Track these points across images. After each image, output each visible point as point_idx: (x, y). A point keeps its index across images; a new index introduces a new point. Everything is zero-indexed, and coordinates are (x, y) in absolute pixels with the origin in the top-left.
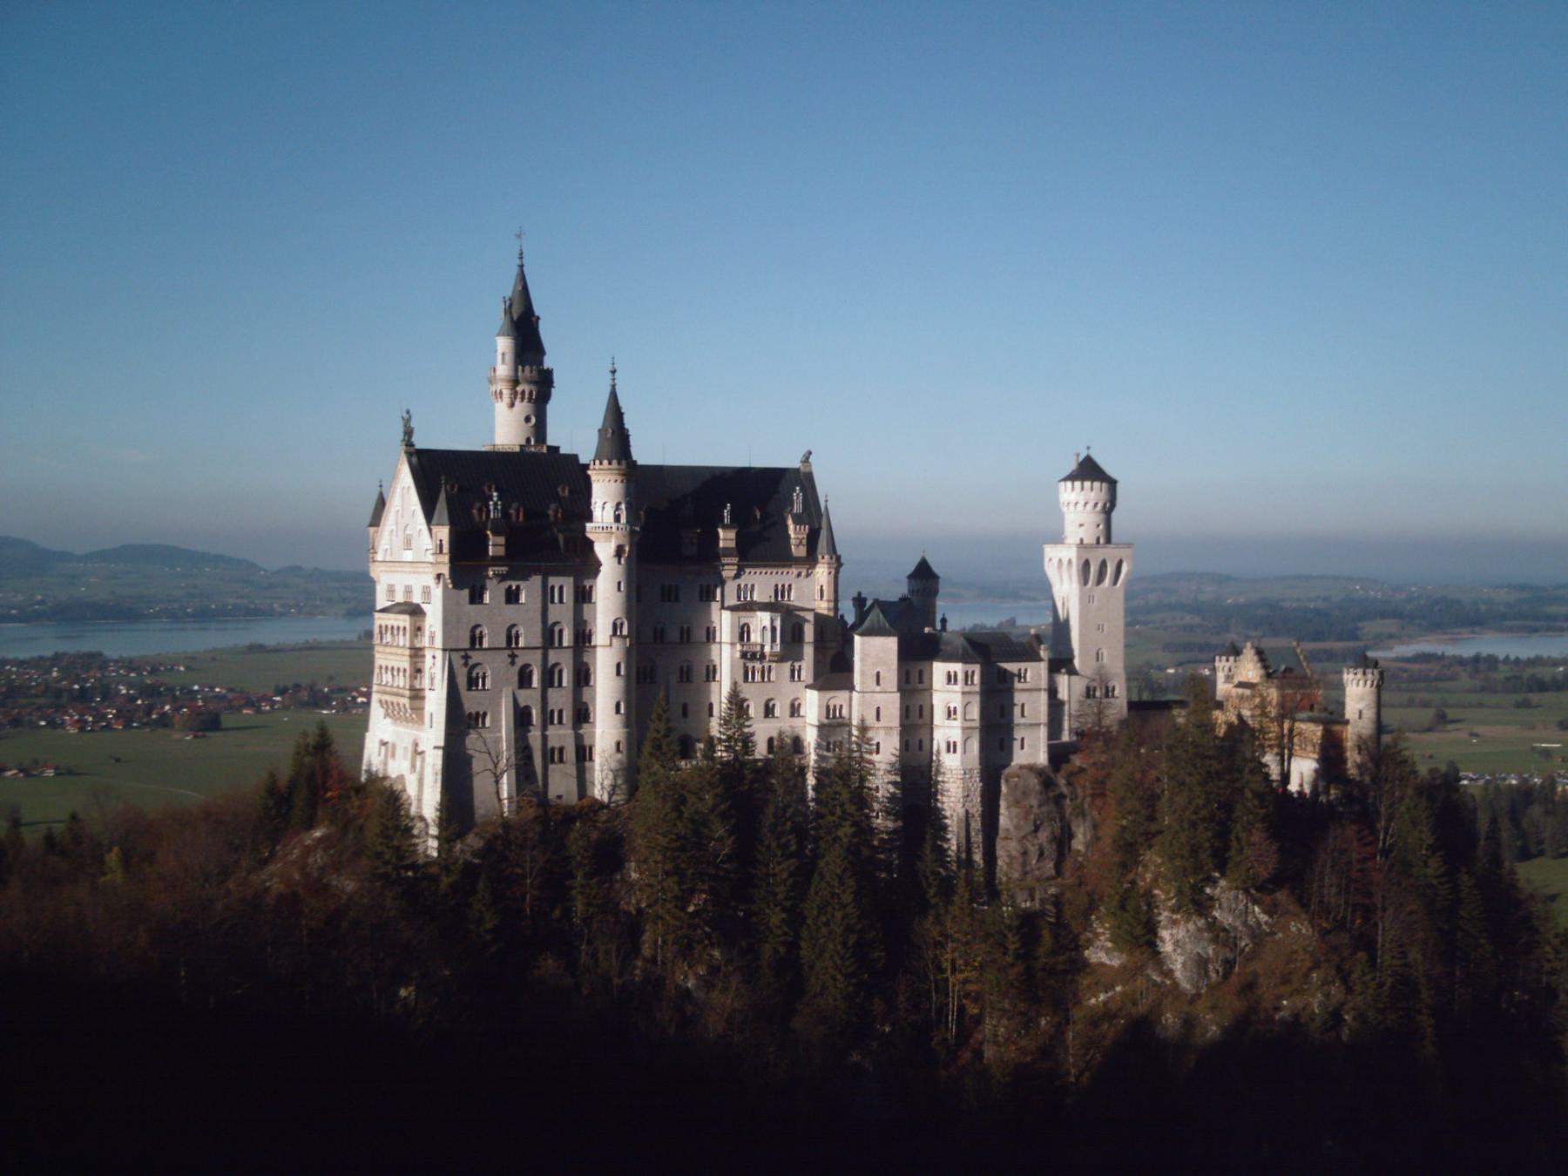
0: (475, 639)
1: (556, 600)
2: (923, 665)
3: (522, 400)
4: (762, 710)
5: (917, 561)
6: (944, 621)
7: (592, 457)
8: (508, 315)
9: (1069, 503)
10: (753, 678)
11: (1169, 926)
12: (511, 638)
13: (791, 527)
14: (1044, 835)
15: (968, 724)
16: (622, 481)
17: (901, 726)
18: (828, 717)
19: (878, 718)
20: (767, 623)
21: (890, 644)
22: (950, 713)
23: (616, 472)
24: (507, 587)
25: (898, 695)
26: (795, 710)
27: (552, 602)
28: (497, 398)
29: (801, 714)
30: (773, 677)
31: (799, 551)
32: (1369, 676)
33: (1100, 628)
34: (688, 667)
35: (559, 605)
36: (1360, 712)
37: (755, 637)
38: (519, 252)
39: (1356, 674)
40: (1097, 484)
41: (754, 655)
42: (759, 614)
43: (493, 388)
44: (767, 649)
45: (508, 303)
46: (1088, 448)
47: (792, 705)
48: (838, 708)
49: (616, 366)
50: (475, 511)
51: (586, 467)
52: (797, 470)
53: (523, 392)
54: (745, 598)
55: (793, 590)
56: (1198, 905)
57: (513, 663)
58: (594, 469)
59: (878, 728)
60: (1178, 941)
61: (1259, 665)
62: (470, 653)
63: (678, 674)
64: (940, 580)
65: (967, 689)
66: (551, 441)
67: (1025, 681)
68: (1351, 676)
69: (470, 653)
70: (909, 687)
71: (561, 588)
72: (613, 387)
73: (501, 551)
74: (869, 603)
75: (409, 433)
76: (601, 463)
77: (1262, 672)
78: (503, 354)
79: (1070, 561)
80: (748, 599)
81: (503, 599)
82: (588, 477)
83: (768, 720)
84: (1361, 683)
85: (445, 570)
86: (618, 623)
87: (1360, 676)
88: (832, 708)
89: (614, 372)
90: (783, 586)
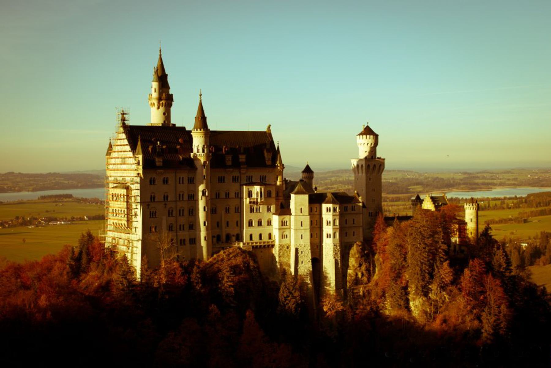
0: (153, 198)
1: (181, 182)
2: (317, 205)
3: (162, 106)
4: (257, 223)
5: (304, 167)
6: (316, 189)
7: (193, 128)
8: (156, 74)
9: (361, 144)
10: (253, 211)
11: (412, 300)
12: (166, 198)
13: (266, 154)
14: (363, 268)
15: (335, 227)
16: (203, 137)
17: (310, 228)
18: (282, 226)
19: (302, 226)
20: (259, 190)
21: (305, 198)
22: (328, 223)
23: (202, 133)
24: (163, 177)
25: (309, 217)
26: (269, 223)
27: (180, 183)
28: (152, 105)
29: (272, 224)
30: (261, 211)
31: (269, 163)
32: (475, 206)
33: (373, 190)
34: (229, 207)
35: (182, 185)
36: (471, 219)
37: (254, 196)
38: (159, 50)
39: (469, 205)
40: (372, 136)
41: (254, 203)
42: (256, 187)
43: (151, 102)
44: (259, 200)
45: (156, 69)
46: (368, 123)
47: (268, 221)
48: (285, 222)
49: (201, 93)
50: (150, 149)
51: (190, 132)
52: (265, 132)
53: (163, 103)
54: (249, 180)
55: (267, 179)
56: (425, 292)
57: (165, 207)
58: (194, 132)
59: (303, 229)
60: (416, 306)
61: (432, 203)
62: (150, 203)
63: (225, 210)
64: (314, 173)
65: (334, 214)
66: (172, 122)
67: (354, 210)
68: (468, 206)
69: (150, 203)
70: (311, 213)
71: (183, 178)
72: (201, 101)
73: (161, 164)
74: (288, 182)
75: (123, 120)
76: (197, 130)
77: (433, 206)
78: (155, 89)
79: (362, 166)
80: (250, 181)
81: (162, 183)
82: (192, 136)
83: (259, 227)
84: (472, 209)
85: (141, 171)
86: (204, 191)
87: (471, 206)
88: (283, 222)
89: (201, 95)
90: (263, 176)
